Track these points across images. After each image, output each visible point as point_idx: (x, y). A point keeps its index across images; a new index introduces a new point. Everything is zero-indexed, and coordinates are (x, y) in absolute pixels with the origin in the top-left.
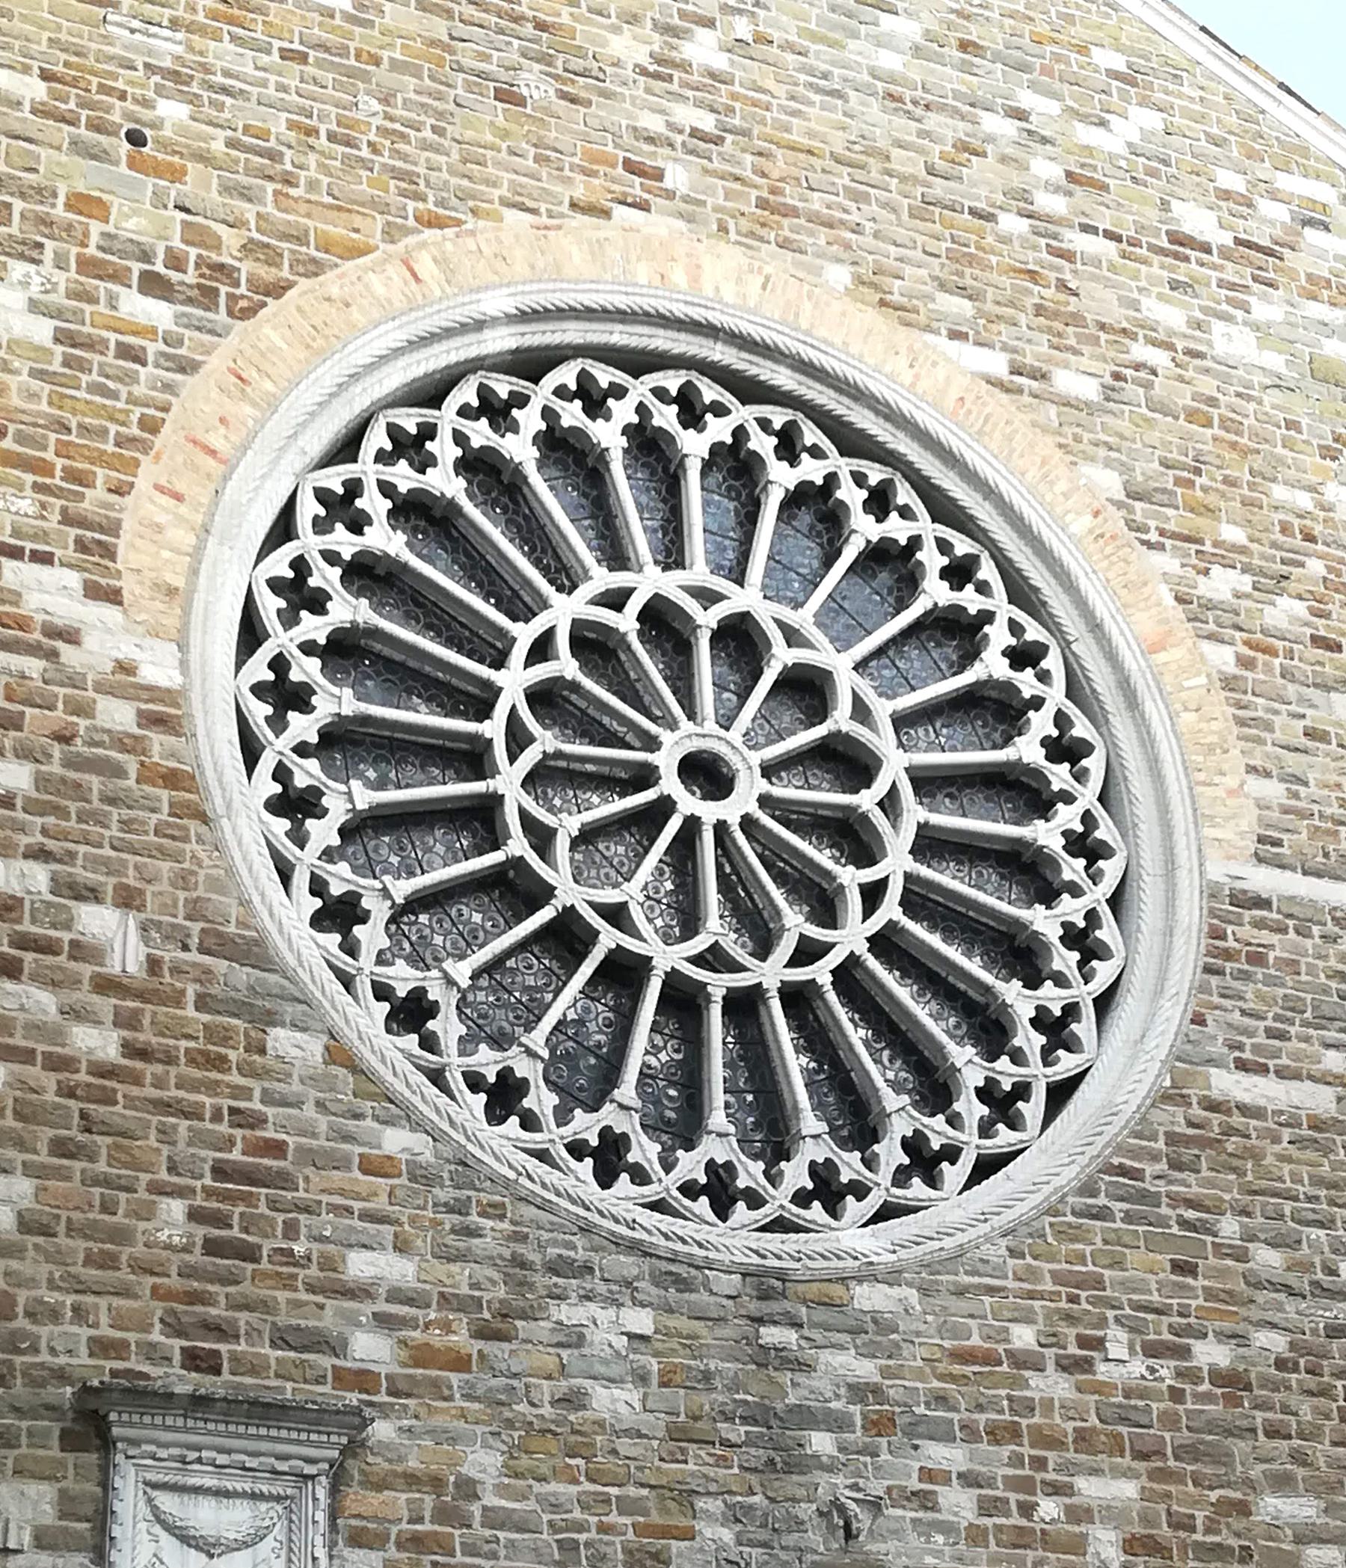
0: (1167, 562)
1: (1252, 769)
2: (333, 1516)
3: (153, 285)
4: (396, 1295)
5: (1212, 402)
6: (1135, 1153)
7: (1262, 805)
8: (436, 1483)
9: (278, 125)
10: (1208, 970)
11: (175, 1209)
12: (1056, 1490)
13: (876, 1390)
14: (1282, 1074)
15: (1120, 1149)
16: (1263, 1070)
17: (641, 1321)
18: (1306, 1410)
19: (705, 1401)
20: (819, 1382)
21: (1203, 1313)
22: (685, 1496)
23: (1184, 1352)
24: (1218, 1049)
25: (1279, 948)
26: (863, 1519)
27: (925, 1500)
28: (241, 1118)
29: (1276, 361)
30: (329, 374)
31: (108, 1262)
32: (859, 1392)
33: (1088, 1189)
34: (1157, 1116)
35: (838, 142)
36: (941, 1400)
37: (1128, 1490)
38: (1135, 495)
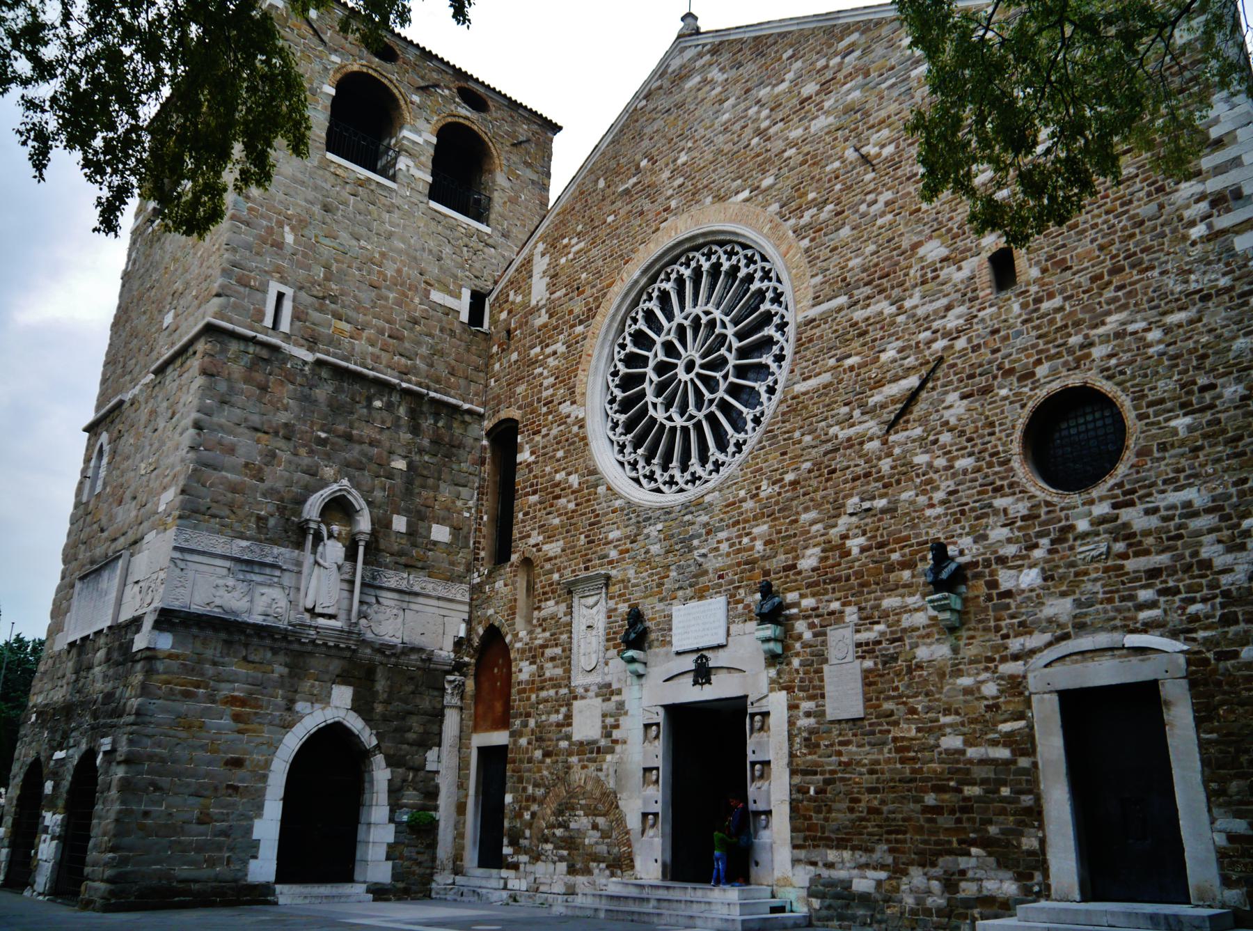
0: (792, 221)
1: (812, 276)
2: (607, 594)
3: (581, 322)
4: (618, 540)
5: (808, 153)
6: (773, 424)
7: (815, 287)
8: (623, 581)
9: (600, 263)
10: (796, 353)
11: (582, 537)
12: (747, 534)
13: (708, 523)
14: (816, 376)
15: (769, 425)
16: (810, 377)
17: (660, 526)
18: (814, 483)
19: (672, 541)
20: (696, 527)
21: (788, 465)
22: (667, 567)
23: (782, 479)
24: (798, 378)
25: (817, 332)
26: (700, 560)
27: (717, 549)
28: (593, 511)
29: (831, 119)
30: (607, 321)
31: (573, 553)
32: (706, 525)
33: (760, 442)
34: (780, 408)
35: (710, 157)
36: (722, 520)
37: (765, 527)
38: (781, 207)
